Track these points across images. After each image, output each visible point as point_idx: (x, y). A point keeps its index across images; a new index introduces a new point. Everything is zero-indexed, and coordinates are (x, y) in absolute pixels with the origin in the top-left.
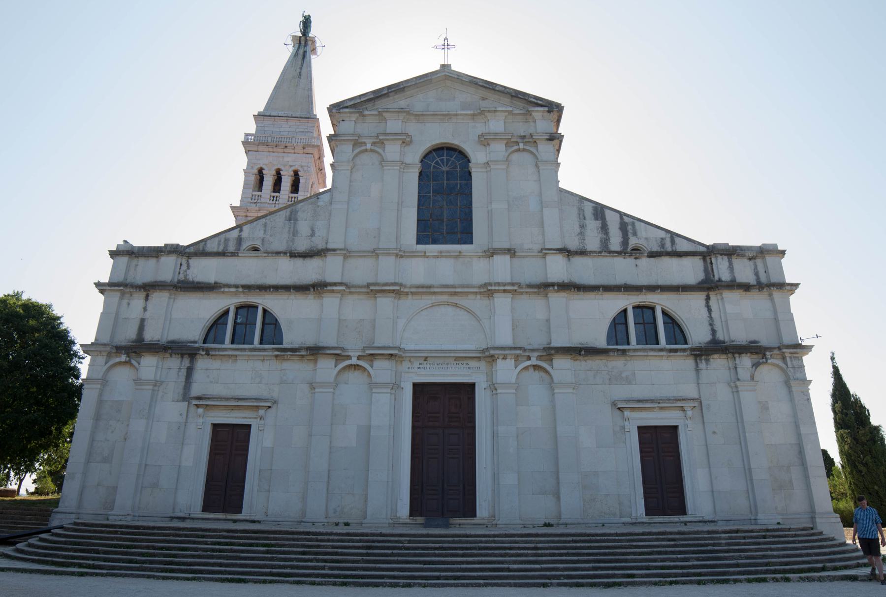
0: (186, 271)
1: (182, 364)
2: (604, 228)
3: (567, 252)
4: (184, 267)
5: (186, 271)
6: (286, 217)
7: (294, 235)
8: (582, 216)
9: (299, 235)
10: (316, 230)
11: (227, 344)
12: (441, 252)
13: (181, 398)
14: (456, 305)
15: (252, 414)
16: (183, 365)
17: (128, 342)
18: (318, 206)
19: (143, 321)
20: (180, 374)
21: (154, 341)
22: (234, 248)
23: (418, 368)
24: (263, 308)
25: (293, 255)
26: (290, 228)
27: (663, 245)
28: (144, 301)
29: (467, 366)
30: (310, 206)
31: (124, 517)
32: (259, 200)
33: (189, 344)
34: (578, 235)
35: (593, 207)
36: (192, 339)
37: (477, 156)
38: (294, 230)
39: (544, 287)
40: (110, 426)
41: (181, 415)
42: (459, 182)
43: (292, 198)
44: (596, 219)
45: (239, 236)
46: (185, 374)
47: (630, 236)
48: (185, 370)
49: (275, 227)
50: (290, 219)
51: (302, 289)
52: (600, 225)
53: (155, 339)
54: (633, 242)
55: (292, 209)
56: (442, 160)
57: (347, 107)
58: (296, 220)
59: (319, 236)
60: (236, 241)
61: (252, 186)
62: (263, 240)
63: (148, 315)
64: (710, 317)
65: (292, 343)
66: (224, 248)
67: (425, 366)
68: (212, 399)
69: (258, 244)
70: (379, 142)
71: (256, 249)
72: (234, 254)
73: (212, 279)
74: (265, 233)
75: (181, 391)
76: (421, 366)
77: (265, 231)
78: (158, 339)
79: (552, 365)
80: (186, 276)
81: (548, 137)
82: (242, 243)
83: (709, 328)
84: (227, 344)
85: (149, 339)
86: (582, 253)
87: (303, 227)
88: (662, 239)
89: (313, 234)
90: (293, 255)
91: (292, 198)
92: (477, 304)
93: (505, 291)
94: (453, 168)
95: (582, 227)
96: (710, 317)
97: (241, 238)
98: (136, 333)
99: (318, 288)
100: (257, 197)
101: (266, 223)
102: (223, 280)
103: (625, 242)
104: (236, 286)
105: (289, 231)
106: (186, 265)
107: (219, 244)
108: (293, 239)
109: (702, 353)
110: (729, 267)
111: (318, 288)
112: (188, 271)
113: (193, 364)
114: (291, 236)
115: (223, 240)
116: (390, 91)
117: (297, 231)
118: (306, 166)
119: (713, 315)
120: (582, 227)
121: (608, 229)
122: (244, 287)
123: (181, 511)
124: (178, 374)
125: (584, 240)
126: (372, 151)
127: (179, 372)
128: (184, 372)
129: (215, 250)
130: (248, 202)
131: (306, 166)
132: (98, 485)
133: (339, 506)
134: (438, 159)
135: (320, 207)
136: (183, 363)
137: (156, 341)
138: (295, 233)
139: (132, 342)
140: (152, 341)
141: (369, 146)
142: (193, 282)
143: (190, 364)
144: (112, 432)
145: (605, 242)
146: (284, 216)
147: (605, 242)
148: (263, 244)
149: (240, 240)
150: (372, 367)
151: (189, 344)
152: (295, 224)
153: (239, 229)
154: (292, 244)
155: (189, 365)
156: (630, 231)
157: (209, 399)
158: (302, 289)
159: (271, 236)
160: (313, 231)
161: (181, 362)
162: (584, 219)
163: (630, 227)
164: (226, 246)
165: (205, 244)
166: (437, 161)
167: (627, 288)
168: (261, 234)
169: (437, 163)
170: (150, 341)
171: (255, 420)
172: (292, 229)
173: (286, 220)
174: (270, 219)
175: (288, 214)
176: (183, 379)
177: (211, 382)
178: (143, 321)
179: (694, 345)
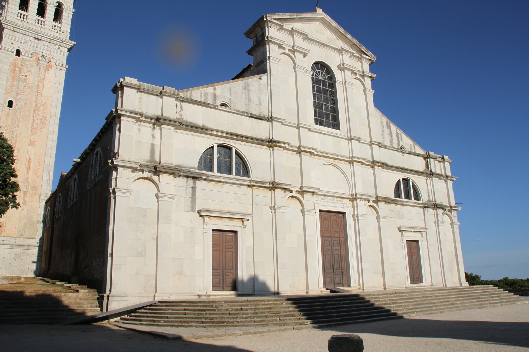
0: (180, 112)
1: (187, 184)
2: (391, 133)
3: (380, 145)
4: (179, 107)
5: (180, 112)
6: (242, 87)
7: (249, 101)
8: (382, 125)
9: (252, 102)
10: (261, 101)
11: (215, 173)
12: (329, 132)
13: (191, 210)
14: (335, 166)
15: (240, 223)
16: (188, 185)
17: (144, 162)
18: (261, 84)
19: (153, 146)
20: (187, 191)
21: (168, 164)
22: (212, 102)
23: (321, 201)
24: (235, 150)
25: (252, 116)
26: (246, 95)
27: (411, 149)
28: (152, 129)
29: (342, 202)
30: (256, 83)
31: (168, 297)
32: (25, 20)
33: (191, 170)
34: (381, 136)
35: (386, 121)
36: (193, 166)
37: (338, 76)
38: (248, 98)
39: (374, 164)
40: (140, 228)
41: (192, 222)
42: (328, 89)
43: (55, 26)
44: (388, 128)
45: (214, 93)
46: (191, 192)
47: (400, 141)
48: (191, 189)
49: (237, 92)
50: (245, 90)
51: (260, 142)
52: (389, 132)
53: (168, 162)
54: (401, 145)
55: (246, 82)
56: (319, 72)
57: (274, 19)
58: (249, 90)
59: (264, 106)
60: (212, 96)
61: (19, 5)
62: (230, 99)
63: (157, 141)
64: (428, 188)
65: (257, 178)
66: (205, 99)
67: (324, 200)
68: (216, 212)
69: (227, 101)
70: (293, 51)
71: (224, 105)
72: (215, 107)
73: (200, 122)
74: (231, 95)
75: (190, 205)
76: (322, 200)
77: (230, 93)
78: (171, 163)
79: (378, 206)
80: (181, 115)
81: (370, 76)
82: (217, 99)
83: (427, 194)
84: (215, 173)
85: (164, 162)
86: (385, 147)
87: (254, 96)
88: (411, 145)
89: (260, 104)
90: (252, 116)
91: (55, 26)
92: (345, 166)
93: (359, 162)
94: (324, 79)
95: (383, 131)
96: (428, 188)
97: (216, 95)
98: (149, 155)
99: (271, 143)
100: (22, 16)
101: (230, 87)
102: (209, 125)
103: (398, 144)
104: (223, 132)
105: (246, 97)
106: (180, 107)
107: (201, 96)
108: (249, 104)
109: (426, 207)
110: (434, 165)
111: (271, 143)
112: (181, 112)
113: (196, 185)
114: (247, 101)
115: (203, 94)
116: (297, 17)
117: (251, 99)
118: (68, 2)
119: (428, 187)
120: (383, 131)
121: (392, 135)
122: (227, 133)
123: (200, 291)
124: (186, 191)
125: (384, 139)
126: (288, 55)
127: (186, 189)
128: (190, 190)
129: (199, 100)
130: (15, 18)
131: (68, 2)
132: (137, 274)
133: (292, 283)
134: (317, 71)
135: (262, 85)
136: (188, 183)
137: (170, 164)
138: (249, 100)
139: (147, 162)
140: (167, 164)
141: (287, 51)
142: (187, 121)
143: (193, 184)
144: (142, 233)
145: (391, 142)
146: (241, 86)
147: (391, 142)
148: (230, 102)
149: (215, 96)
150: (303, 198)
151: (191, 170)
152: (249, 93)
153: (213, 87)
154: (248, 107)
155: (193, 185)
156: (400, 138)
157: (214, 211)
158: (260, 142)
159: (235, 98)
160: (260, 101)
161: (187, 182)
162: (383, 127)
163: (400, 136)
164: (206, 98)
165: (191, 93)
166: (317, 72)
167: (404, 170)
168: (228, 95)
169: (316, 72)
170: (165, 163)
171: (240, 228)
172: (247, 97)
173: (243, 89)
174: (232, 85)
175: (244, 85)
176: (190, 195)
177: (208, 200)
178: (153, 146)
179: (424, 202)
